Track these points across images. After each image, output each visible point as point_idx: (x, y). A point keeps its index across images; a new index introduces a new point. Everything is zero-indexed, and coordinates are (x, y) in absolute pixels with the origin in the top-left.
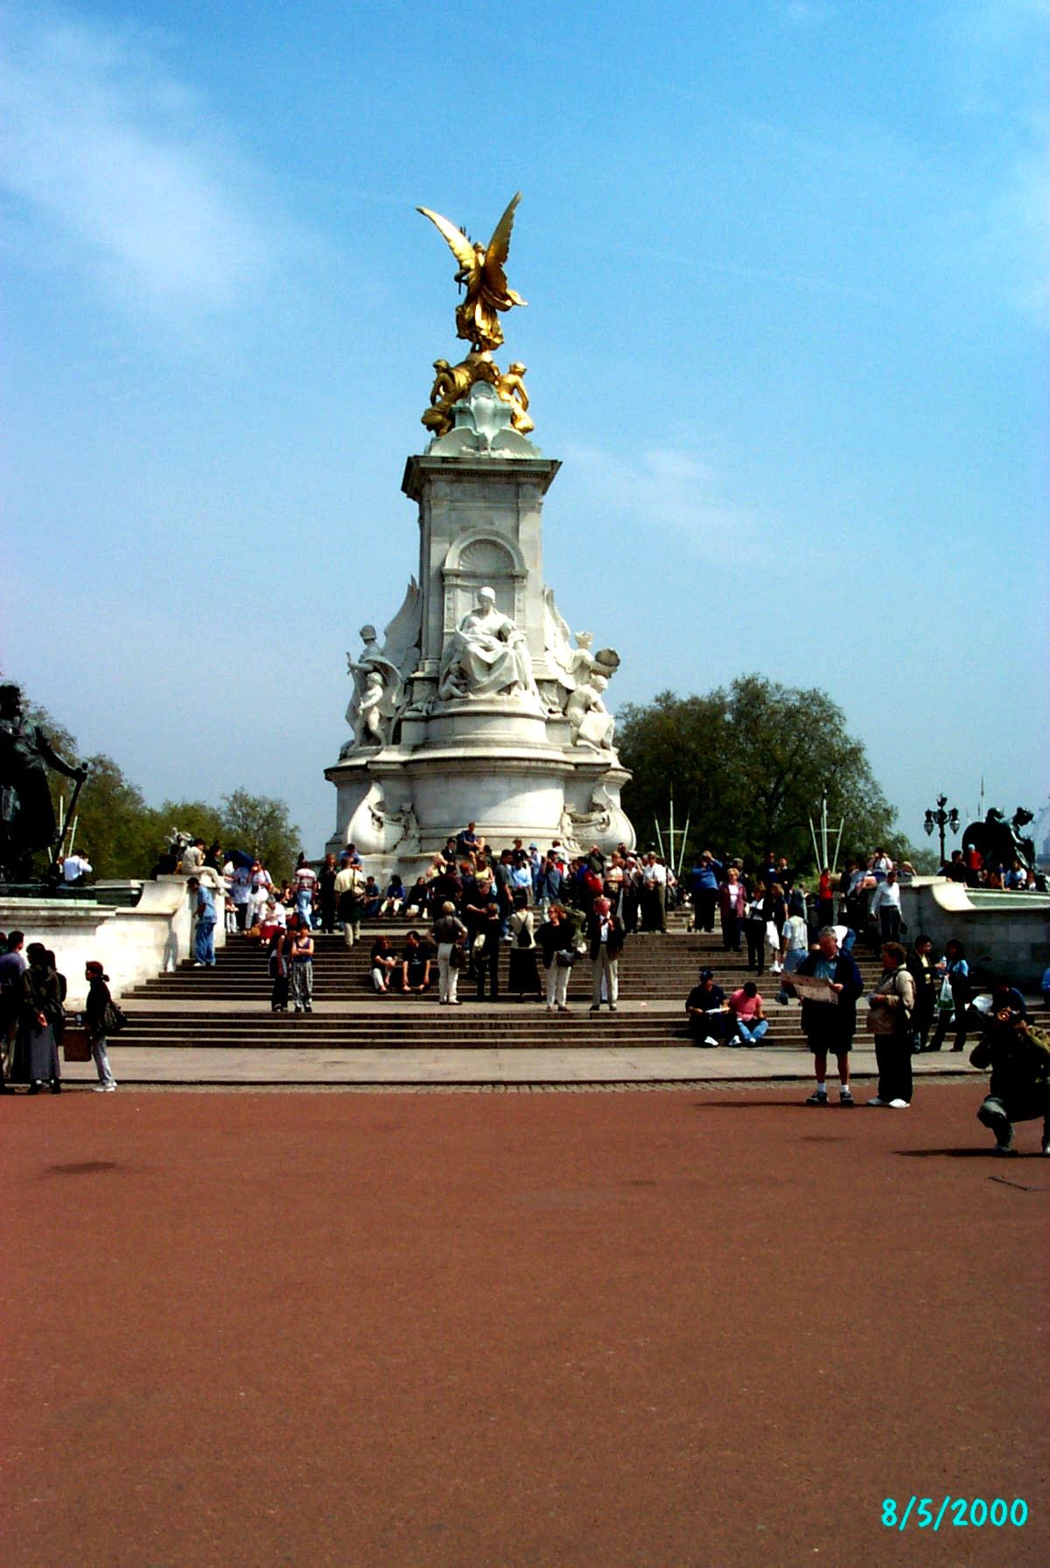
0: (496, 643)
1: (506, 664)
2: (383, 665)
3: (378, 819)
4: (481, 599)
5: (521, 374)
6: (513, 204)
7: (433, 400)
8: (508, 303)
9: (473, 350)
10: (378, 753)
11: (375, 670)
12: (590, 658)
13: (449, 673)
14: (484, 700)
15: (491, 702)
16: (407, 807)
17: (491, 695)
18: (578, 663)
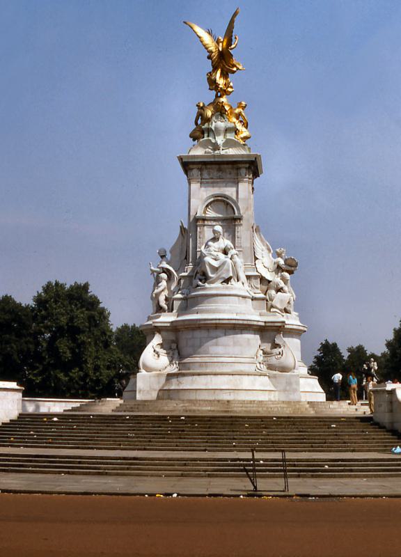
0: (222, 256)
1: (225, 267)
2: (168, 270)
3: (157, 353)
4: (214, 232)
5: (243, 108)
6: (235, 14)
7: (196, 123)
8: (235, 69)
9: (217, 96)
10: (159, 317)
11: (164, 272)
12: (282, 262)
13: (197, 273)
14: (214, 287)
15: (217, 288)
16: (174, 346)
17: (218, 284)
18: (276, 266)
